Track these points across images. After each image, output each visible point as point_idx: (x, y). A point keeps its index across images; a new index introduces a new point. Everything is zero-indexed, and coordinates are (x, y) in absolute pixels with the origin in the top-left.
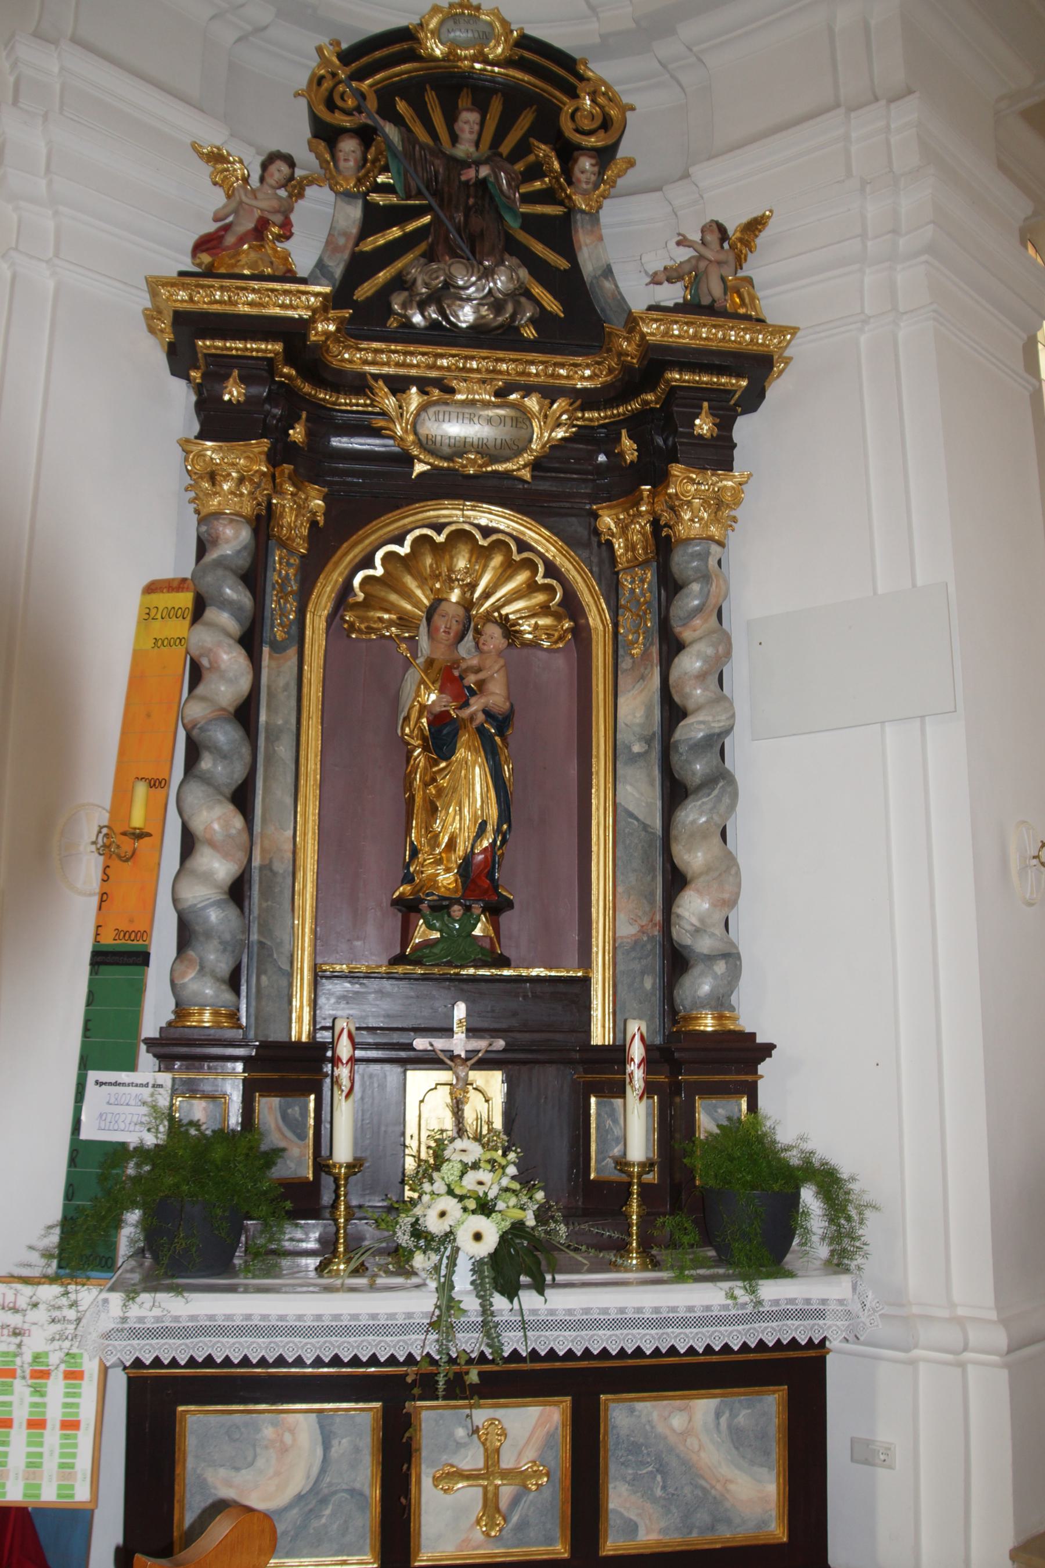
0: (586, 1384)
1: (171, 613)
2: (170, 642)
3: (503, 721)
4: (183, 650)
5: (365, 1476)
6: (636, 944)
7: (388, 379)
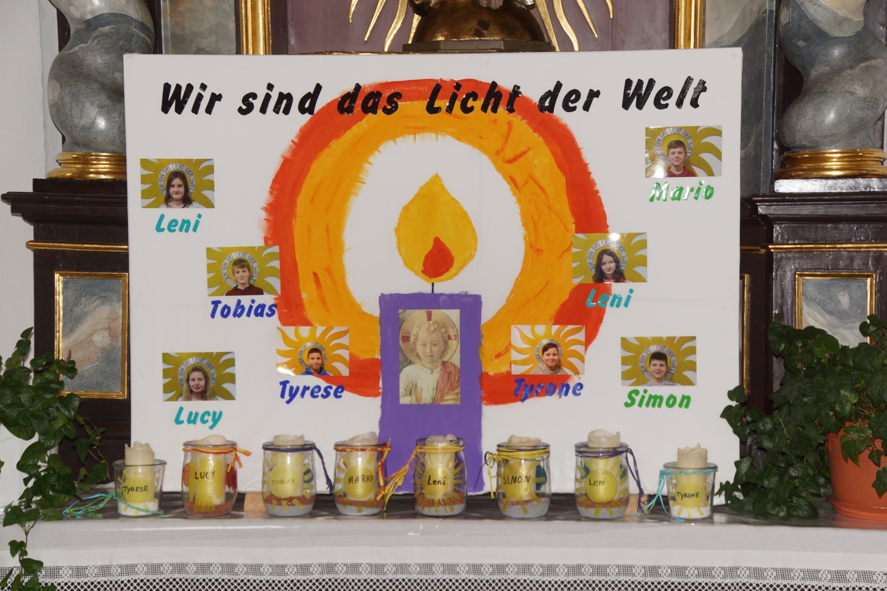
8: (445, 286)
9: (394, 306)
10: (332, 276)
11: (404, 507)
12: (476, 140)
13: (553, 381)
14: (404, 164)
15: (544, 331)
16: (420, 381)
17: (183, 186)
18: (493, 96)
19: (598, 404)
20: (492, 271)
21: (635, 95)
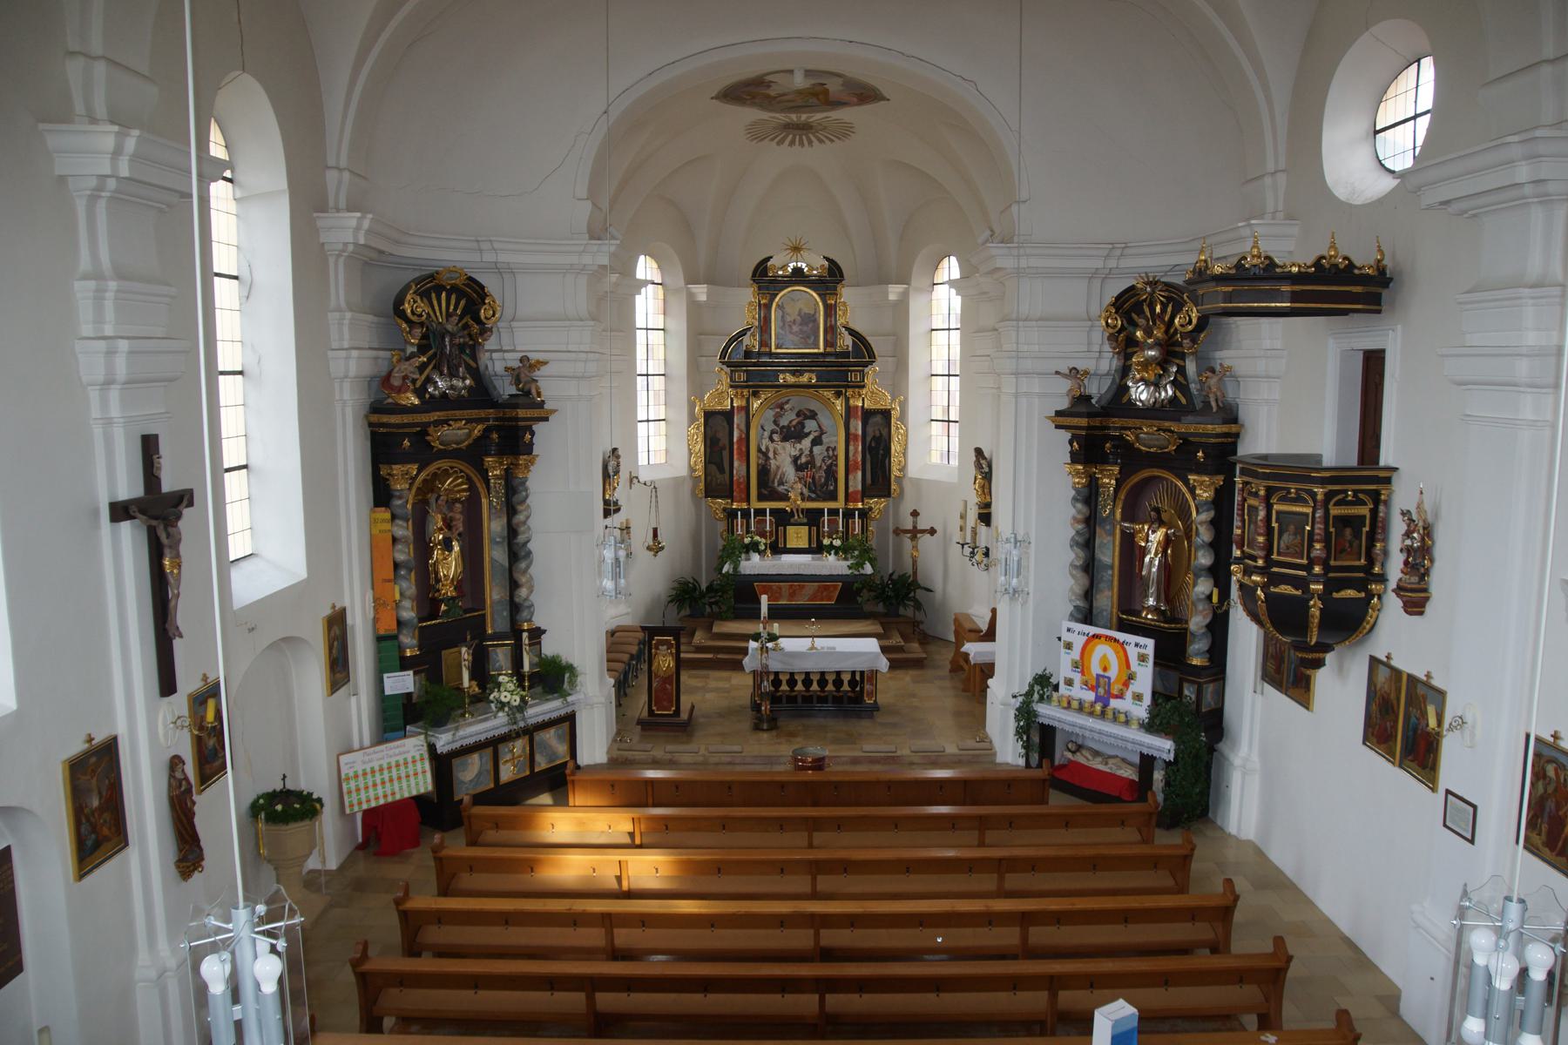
0: (530, 732)
1: (383, 521)
5: (490, 766)
6: (499, 602)
11: (1091, 714)
13: (1120, 696)
14: (1102, 650)
16: (1101, 691)
18: (1116, 640)
20: (1113, 673)
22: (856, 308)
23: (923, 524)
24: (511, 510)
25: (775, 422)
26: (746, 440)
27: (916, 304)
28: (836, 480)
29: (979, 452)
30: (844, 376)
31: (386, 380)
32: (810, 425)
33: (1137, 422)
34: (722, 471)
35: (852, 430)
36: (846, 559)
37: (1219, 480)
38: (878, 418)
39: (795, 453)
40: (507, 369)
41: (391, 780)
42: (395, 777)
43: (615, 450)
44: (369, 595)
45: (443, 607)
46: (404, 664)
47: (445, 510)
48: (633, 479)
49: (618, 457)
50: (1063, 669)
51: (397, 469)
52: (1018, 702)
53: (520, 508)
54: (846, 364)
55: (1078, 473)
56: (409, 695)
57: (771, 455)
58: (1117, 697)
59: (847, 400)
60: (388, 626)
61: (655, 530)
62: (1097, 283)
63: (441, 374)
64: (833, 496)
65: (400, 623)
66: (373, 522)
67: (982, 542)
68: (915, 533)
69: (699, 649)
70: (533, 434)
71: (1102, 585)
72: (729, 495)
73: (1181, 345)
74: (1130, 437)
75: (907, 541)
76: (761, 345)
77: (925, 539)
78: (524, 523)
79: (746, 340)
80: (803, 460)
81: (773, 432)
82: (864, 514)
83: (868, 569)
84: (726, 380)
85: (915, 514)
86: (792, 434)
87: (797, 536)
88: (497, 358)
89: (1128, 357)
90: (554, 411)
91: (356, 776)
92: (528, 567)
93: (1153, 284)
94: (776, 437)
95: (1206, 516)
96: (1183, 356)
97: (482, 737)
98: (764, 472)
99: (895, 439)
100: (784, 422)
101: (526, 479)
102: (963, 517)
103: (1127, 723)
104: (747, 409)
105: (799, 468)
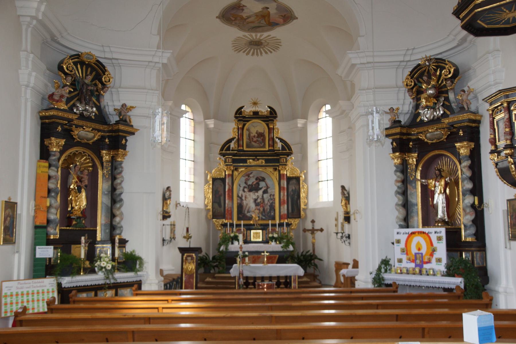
1: (44, 167)
2: (45, 172)
3: (86, 186)
4: (47, 174)
7: (75, 125)
8: (420, 252)
9: (416, 254)
10: (410, 250)
11: (414, 274)
12: (421, 236)
13: (429, 262)
14: (417, 239)
15: (428, 257)
16: (418, 262)
17: (398, 242)
18: (424, 233)
19: (433, 265)
20: (424, 251)
21: (436, 232)
22: (282, 129)
23: (317, 226)
24: (114, 178)
25: (246, 183)
26: (231, 190)
27: (310, 129)
28: (274, 210)
29: (343, 188)
30: (278, 161)
31: (51, 96)
32: (262, 184)
33: (425, 129)
34: (220, 206)
35: (282, 185)
36: (280, 243)
37: (473, 145)
38: (294, 181)
39: (255, 197)
40: (115, 110)
41: (33, 301)
42: (36, 299)
43: (168, 188)
44: (32, 203)
45: (74, 223)
46: (49, 242)
47: (79, 173)
48: (177, 204)
49: (170, 191)
50: (397, 253)
51: (53, 140)
52: (373, 276)
53: (118, 176)
54: (278, 155)
55: (397, 158)
56: (50, 259)
57: (244, 198)
58: (427, 263)
59: (279, 171)
60: (42, 221)
61: (188, 229)
62: (400, 70)
63: (81, 103)
64: (274, 218)
65: (49, 221)
66: (38, 167)
67: (347, 233)
68: (313, 231)
69: (208, 283)
70: (126, 141)
71: (413, 214)
72: (224, 217)
73: (445, 86)
74: (422, 137)
75: (309, 235)
76: (238, 147)
77: (318, 234)
78: (120, 184)
79: (232, 145)
80: (259, 200)
81: (245, 187)
82: (288, 225)
83: (291, 248)
84: (222, 164)
85: (313, 222)
86: (254, 188)
87: (256, 235)
88: (111, 102)
89: (417, 99)
90: (137, 130)
91: (12, 295)
92: (121, 206)
93: (429, 60)
94: (246, 190)
95: (467, 163)
96: (447, 92)
97: (89, 284)
98: (240, 207)
99: (302, 190)
100: (250, 183)
101: (121, 163)
102: (336, 220)
103: (434, 275)
104: (232, 175)
105: (257, 204)
